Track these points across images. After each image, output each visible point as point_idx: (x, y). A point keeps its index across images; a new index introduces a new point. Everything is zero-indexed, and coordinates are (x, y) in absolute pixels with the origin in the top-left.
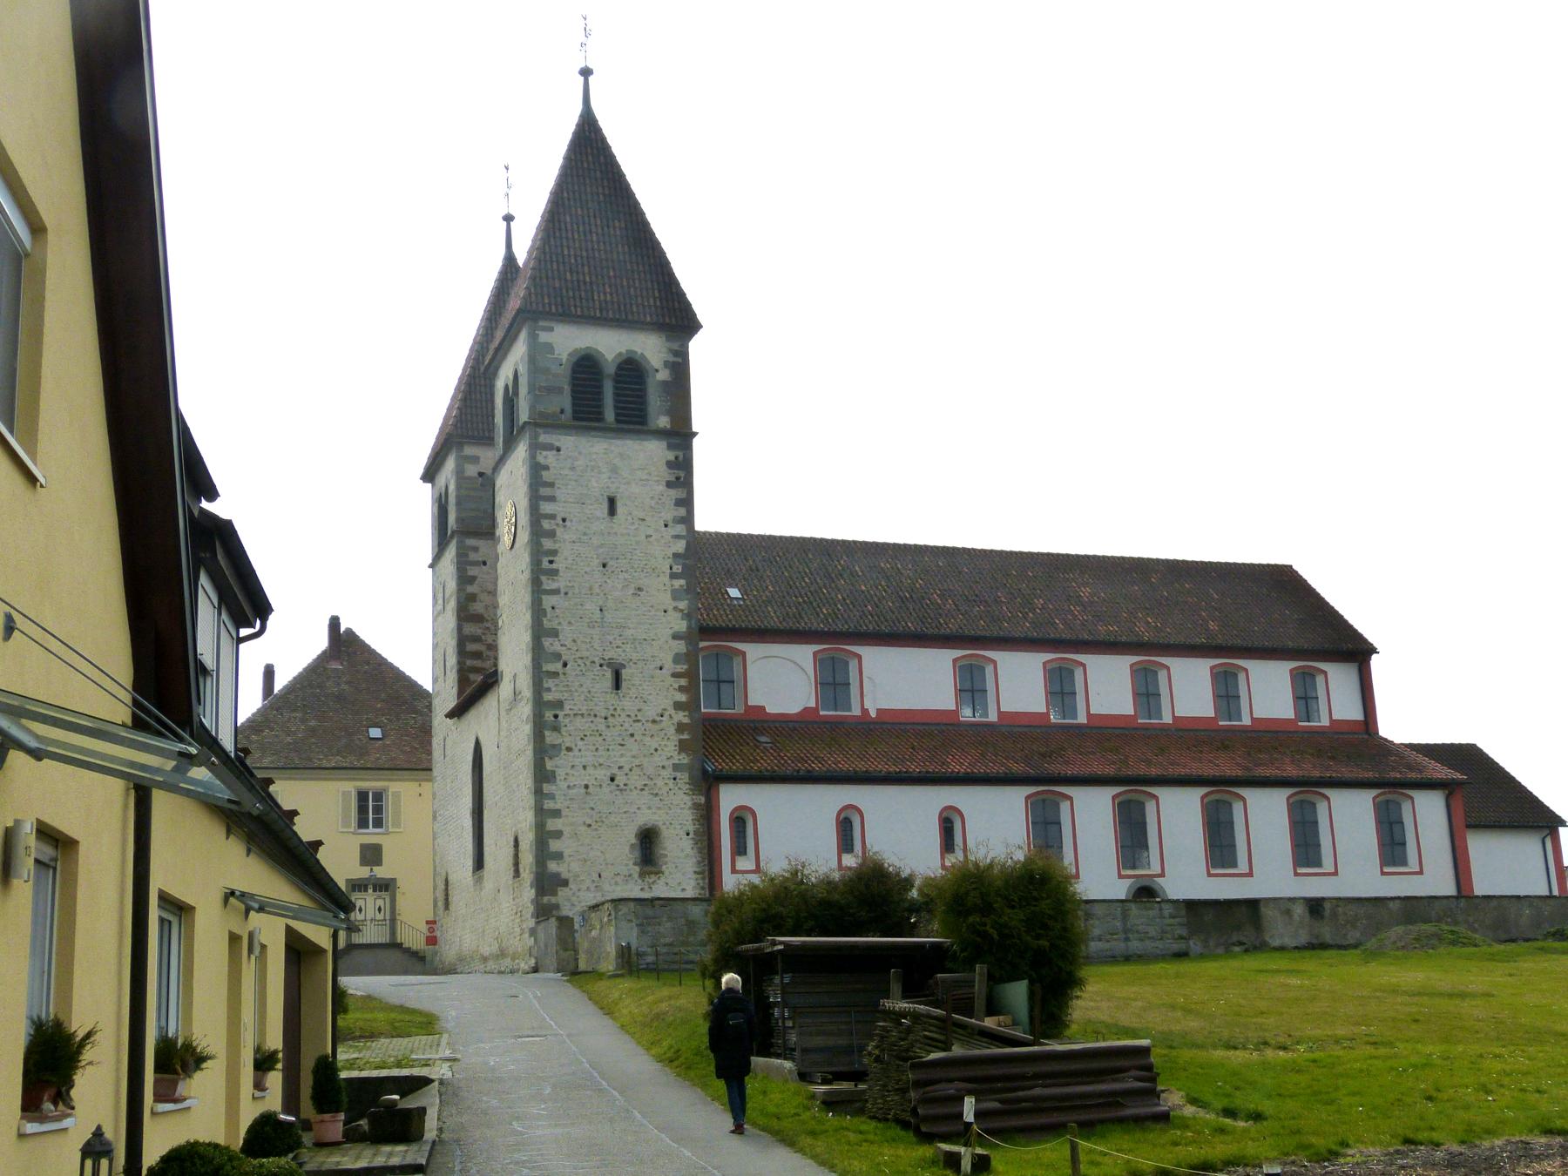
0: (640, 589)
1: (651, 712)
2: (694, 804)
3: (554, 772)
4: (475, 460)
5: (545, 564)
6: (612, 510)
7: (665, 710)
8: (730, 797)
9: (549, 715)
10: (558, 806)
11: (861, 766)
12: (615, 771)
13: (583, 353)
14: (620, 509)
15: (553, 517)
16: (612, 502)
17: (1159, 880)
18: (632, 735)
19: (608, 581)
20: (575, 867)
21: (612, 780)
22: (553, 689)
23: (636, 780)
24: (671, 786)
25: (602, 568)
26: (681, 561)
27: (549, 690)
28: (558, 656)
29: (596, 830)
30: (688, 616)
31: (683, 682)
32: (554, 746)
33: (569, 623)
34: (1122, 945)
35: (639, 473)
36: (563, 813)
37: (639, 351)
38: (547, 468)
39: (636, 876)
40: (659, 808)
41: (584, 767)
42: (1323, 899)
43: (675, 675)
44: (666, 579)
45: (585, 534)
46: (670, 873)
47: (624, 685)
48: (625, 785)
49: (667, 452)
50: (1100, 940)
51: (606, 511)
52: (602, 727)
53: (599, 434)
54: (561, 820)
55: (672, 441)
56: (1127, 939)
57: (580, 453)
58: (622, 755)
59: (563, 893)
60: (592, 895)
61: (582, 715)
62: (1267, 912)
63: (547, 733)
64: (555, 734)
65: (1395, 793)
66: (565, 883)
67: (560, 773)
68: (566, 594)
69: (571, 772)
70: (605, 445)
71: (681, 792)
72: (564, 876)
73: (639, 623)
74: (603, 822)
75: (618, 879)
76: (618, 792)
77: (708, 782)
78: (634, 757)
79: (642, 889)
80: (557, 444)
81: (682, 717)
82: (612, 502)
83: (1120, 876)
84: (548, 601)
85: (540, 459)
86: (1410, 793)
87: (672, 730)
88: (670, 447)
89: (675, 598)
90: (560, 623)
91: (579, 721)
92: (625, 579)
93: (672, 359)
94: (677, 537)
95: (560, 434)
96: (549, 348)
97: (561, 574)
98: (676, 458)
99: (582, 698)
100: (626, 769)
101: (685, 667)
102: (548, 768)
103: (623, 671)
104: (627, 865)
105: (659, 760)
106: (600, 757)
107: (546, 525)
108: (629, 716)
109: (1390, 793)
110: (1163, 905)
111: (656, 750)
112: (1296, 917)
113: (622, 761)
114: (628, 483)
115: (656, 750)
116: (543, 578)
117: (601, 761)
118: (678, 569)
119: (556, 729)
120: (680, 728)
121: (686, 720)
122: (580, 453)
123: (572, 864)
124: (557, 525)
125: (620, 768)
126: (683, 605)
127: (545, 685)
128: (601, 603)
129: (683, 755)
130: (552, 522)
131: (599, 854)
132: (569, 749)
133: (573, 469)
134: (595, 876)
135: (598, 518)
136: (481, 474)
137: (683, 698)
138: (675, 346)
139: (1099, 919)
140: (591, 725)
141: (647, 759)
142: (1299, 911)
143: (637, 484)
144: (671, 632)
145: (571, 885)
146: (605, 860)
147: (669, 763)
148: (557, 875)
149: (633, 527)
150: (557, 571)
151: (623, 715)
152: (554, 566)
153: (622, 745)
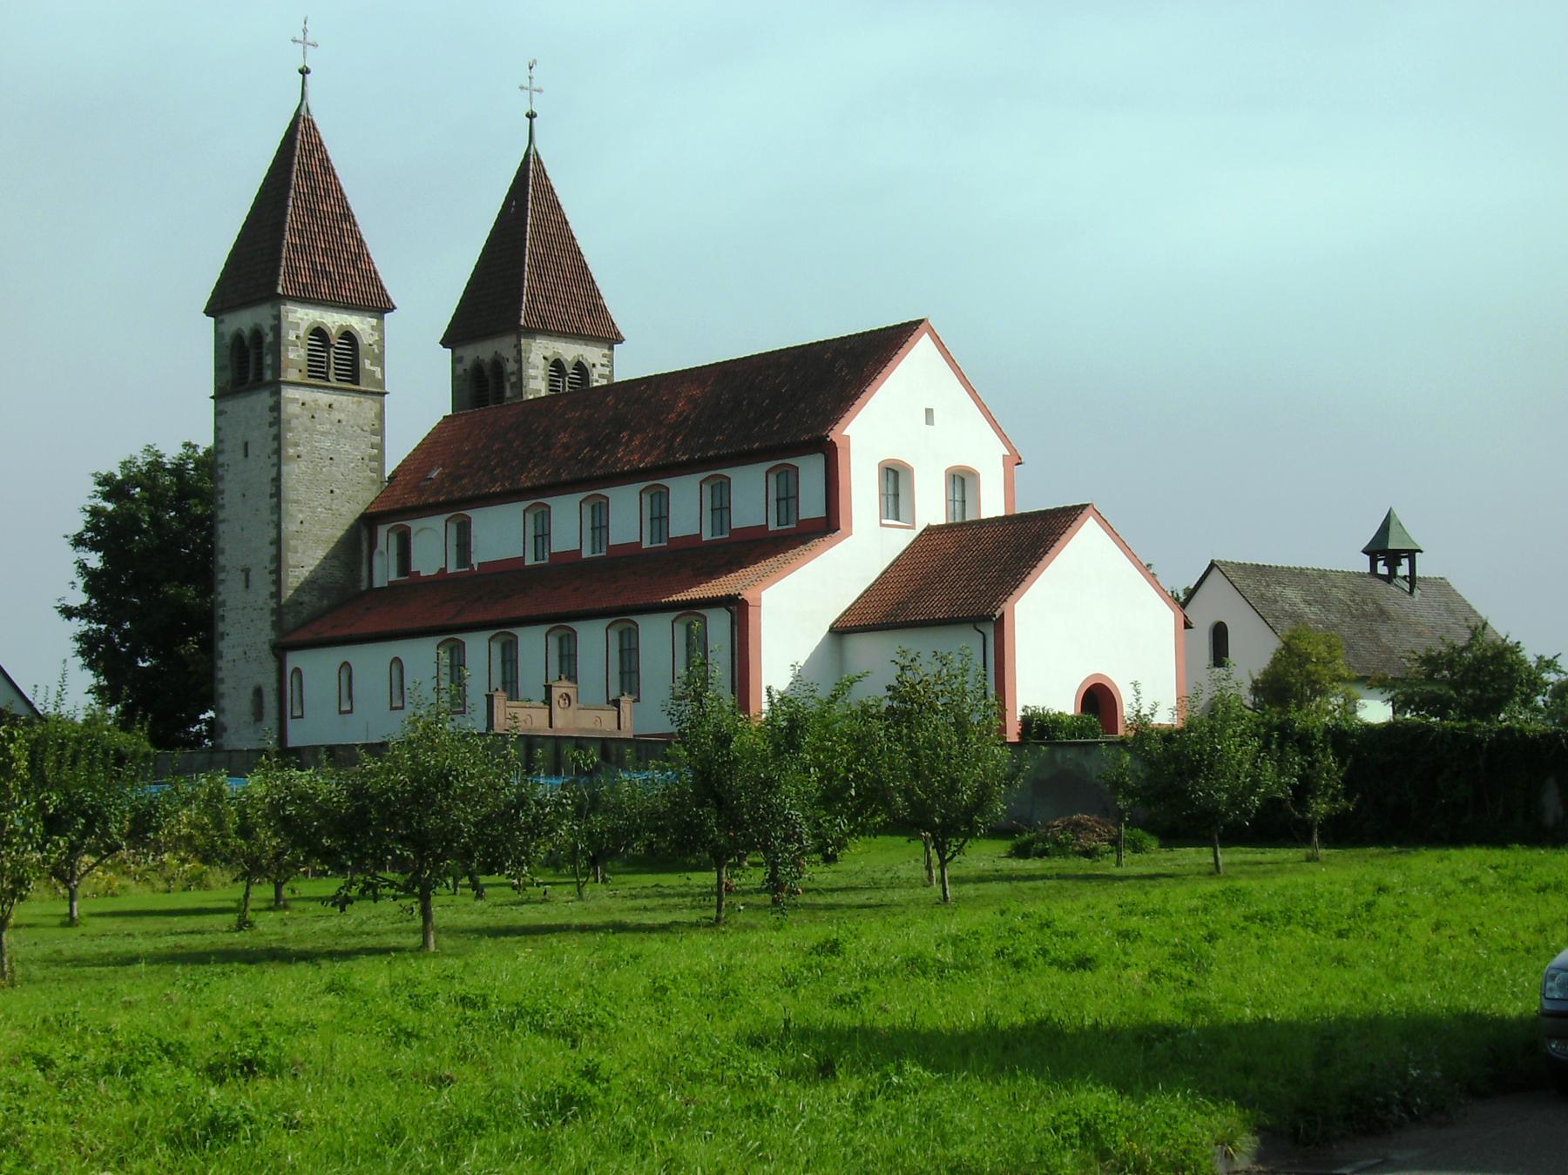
8: (294, 660)
16: (246, 444)
37: (259, 322)
43: (271, 573)
44: (268, 499)
77: (280, 650)
85: (218, 424)
94: (273, 465)
138: (275, 313)
144: (269, 539)
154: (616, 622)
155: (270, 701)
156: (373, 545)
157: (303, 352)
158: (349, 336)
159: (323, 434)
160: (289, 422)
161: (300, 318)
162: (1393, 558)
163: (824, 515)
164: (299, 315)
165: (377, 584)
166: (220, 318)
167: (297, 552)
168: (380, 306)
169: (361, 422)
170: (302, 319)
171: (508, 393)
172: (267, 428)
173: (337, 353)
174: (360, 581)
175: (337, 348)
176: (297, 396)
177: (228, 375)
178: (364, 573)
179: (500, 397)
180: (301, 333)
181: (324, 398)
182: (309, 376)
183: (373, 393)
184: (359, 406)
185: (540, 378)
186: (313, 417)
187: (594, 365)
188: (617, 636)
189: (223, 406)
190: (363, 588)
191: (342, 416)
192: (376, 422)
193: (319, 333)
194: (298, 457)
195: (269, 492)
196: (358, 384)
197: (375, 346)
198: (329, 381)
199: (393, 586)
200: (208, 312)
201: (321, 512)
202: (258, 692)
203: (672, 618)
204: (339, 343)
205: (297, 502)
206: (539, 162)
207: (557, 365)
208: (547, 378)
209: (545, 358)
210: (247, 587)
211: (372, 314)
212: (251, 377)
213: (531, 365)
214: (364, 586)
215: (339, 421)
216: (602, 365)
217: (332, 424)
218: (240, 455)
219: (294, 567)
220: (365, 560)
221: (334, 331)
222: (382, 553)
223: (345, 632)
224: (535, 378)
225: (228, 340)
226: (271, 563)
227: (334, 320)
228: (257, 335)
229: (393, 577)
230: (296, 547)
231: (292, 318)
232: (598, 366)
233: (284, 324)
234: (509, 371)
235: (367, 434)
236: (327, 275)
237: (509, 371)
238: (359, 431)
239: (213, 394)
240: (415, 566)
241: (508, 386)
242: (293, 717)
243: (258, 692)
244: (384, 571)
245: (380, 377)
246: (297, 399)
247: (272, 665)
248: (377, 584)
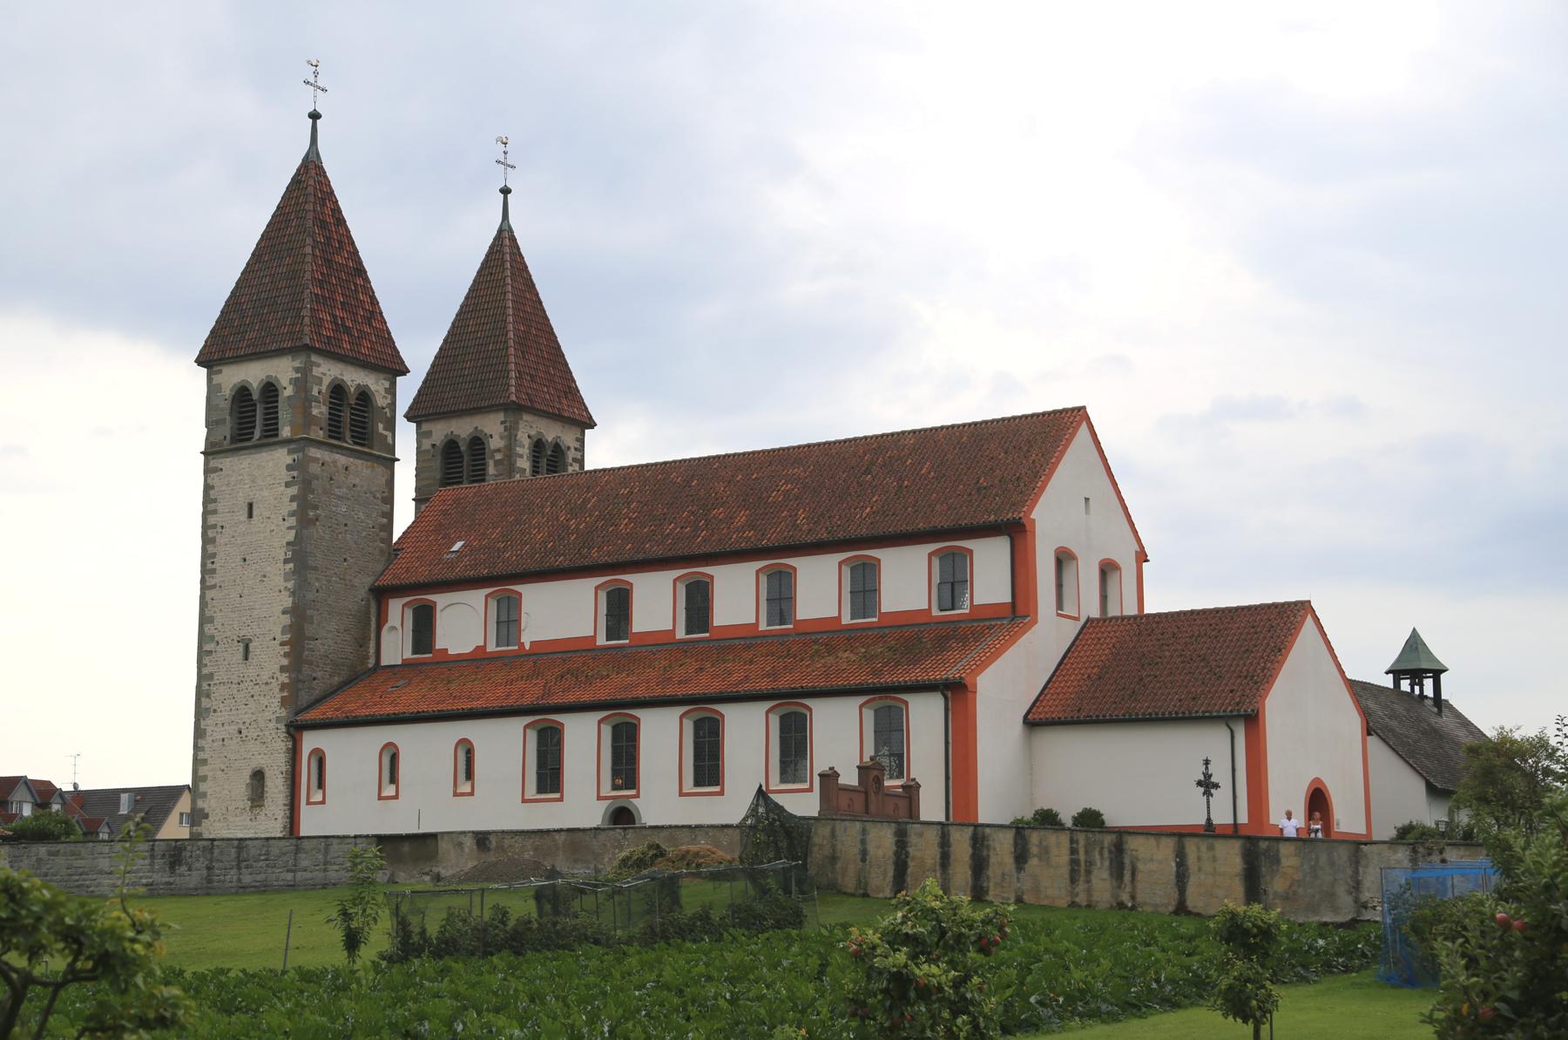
0: (265, 576)
1: (265, 677)
2: (287, 749)
3: (205, 729)
4: (428, 434)
5: (209, 566)
6: (250, 516)
7: (274, 673)
8: (310, 741)
9: (205, 686)
10: (206, 756)
11: (364, 712)
12: (241, 726)
13: (239, 386)
14: (255, 513)
15: (214, 526)
16: (250, 506)
17: (634, 801)
18: (252, 696)
19: (246, 572)
20: (213, 803)
21: (240, 732)
22: (209, 664)
23: (253, 733)
24: (274, 735)
25: (242, 563)
26: (291, 548)
27: (206, 665)
28: (212, 638)
29: (227, 774)
30: (293, 594)
31: (287, 649)
32: (206, 709)
33: (221, 610)
34: (321, 875)
35: (269, 478)
36: (209, 762)
38: (212, 487)
39: (248, 809)
40: (265, 754)
41: (223, 724)
42: (489, 833)
44: (281, 565)
45: (233, 537)
46: (269, 806)
47: (251, 655)
48: (246, 736)
49: (287, 457)
50: (305, 870)
51: (246, 515)
52: (235, 692)
53: (245, 452)
54: (206, 768)
55: (293, 446)
56: (325, 870)
57: (233, 471)
58: (246, 713)
59: (205, 823)
60: (221, 825)
61: (224, 683)
62: (443, 845)
63: (203, 699)
64: (208, 700)
65: (886, 698)
66: (206, 816)
67: (209, 730)
68: (220, 587)
69: (215, 729)
70: (249, 460)
71: (280, 740)
72: (206, 811)
73: (263, 604)
74: (231, 767)
75: (238, 811)
76: (241, 743)
77: (295, 730)
78: (252, 714)
79: (251, 819)
80: (220, 467)
81: (284, 678)
82: (250, 506)
83: (599, 798)
84: (210, 594)
85: (209, 481)
86: (906, 699)
87: (277, 690)
88: (290, 452)
89: (286, 580)
90: (215, 612)
91: (222, 688)
92: (256, 569)
93: (295, 375)
95: (223, 458)
96: (219, 386)
97: (217, 572)
98: (294, 461)
99: (225, 669)
100: (247, 724)
101: (289, 636)
102: (202, 727)
103: (251, 645)
104: (243, 800)
105: (268, 715)
106: (233, 715)
107: (211, 533)
108: (251, 681)
109: (880, 698)
110: (358, 841)
111: (266, 707)
112: (467, 850)
113: (246, 718)
114: (261, 490)
115: (266, 707)
116: (207, 577)
117: (233, 718)
118: (290, 554)
119: (208, 696)
120: (283, 687)
121: (287, 681)
122: (233, 471)
123: (212, 801)
124: (217, 532)
125: (244, 723)
126: (290, 585)
127: (204, 662)
128: (240, 592)
129: (283, 709)
130: (215, 530)
131: (228, 793)
132: (215, 711)
133: (228, 485)
134: (224, 809)
135: (242, 522)
136: (434, 445)
137: (285, 662)
139: (306, 853)
140: (228, 690)
141: (260, 715)
142: (469, 843)
143: (267, 489)
144: (282, 608)
145: (210, 818)
146: (230, 797)
147: (273, 717)
148: (203, 809)
149: (262, 526)
150: (215, 569)
151: (248, 680)
152: (214, 566)
153: (246, 705)
154: (874, 699)
155: (276, 787)
156: (382, 619)
157: (324, 409)
158: (364, 396)
159: (339, 498)
160: (311, 481)
161: (328, 371)
162: (1417, 676)
163: (1008, 599)
164: (321, 370)
165: (385, 662)
166: (215, 369)
167: (312, 623)
168: (395, 368)
169: (373, 490)
170: (325, 375)
171: (491, 470)
172: (283, 488)
173: (352, 414)
174: (368, 658)
175: (352, 408)
176: (319, 456)
177: (226, 430)
178: (372, 650)
179: (479, 475)
180: (324, 388)
181: (342, 460)
182: (330, 437)
183: (384, 458)
184: (372, 471)
185: (525, 457)
186: (331, 479)
187: (569, 448)
188: (778, 719)
189: (213, 463)
190: (370, 666)
191: (357, 481)
192: (386, 490)
193: (338, 390)
194: (317, 520)
195: (282, 557)
196: (371, 448)
197: (387, 410)
198: (347, 442)
199: (407, 664)
200: (200, 361)
201: (336, 582)
202: (258, 776)
203: (599, 718)
204: (356, 404)
205: (315, 569)
206: (513, 239)
207: (538, 445)
208: (531, 459)
209: (529, 437)
210: (246, 658)
211: (386, 376)
212: (257, 434)
213: (518, 443)
214: (371, 662)
215: (354, 486)
216: (576, 449)
217: (349, 488)
218: (243, 516)
219: (310, 639)
220: (373, 635)
221: (352, 390)
222: (394, 628)
223: (389, 710)
224: (521, 456)
225: (227, 392)
226: (283, 634)
227: (354, 378)
228: (270, 389)
229: (408, 654)
230: (312, 617)
231: (316, 371)
232: (573, 450)
233: (310, 379)
234: (492, 448)
235: (379, 502)
236: (347, 330)
237: (492, 448)
238: (372, 498)
239: (203, 450)
240: (440, 644)
241: (491, 463)
242: (308, 803)
243: (258, 776)
244: (396, 646)
245: (391, 442)
246: (318, 459)
247: (280, 745)
248: (385, 662)
